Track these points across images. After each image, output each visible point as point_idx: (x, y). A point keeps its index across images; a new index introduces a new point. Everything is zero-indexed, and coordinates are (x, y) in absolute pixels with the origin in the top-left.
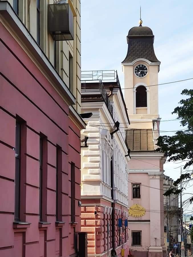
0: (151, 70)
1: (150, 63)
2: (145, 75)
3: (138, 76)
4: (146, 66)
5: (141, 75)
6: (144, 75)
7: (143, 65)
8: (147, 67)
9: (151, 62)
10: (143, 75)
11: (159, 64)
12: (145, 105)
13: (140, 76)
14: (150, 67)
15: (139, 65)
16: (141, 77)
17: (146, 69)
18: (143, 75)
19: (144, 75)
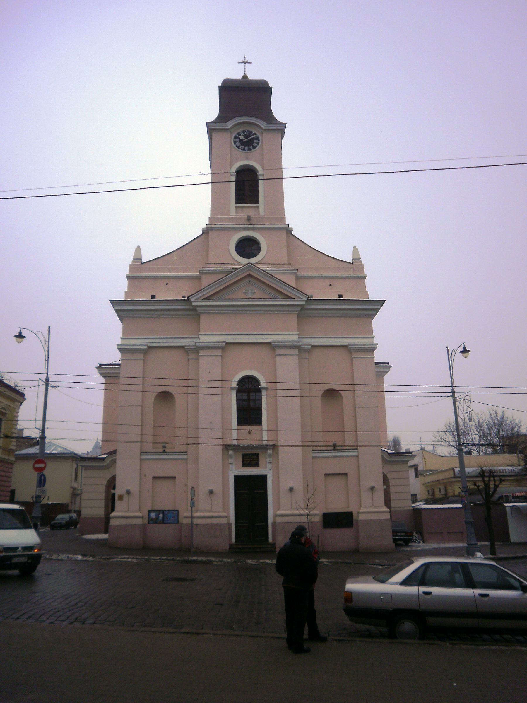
0: (266, 139)
1: (263, 125)
2: (254, 147)
3: (240, 150)
4: (256, 132)
5: (246, 148)
6: (252, 148)
7: (250, 132)
8: (259, 135)
9: (266, 123)
10: (251, 147)
11: (283, 128)
12: (257, 202)
13: (244, 149)
14: (265, 134)
15: (243, 132)
16: (247, 151)
17: (258, 139)
18: (251, 147)
19: (252, 148)
